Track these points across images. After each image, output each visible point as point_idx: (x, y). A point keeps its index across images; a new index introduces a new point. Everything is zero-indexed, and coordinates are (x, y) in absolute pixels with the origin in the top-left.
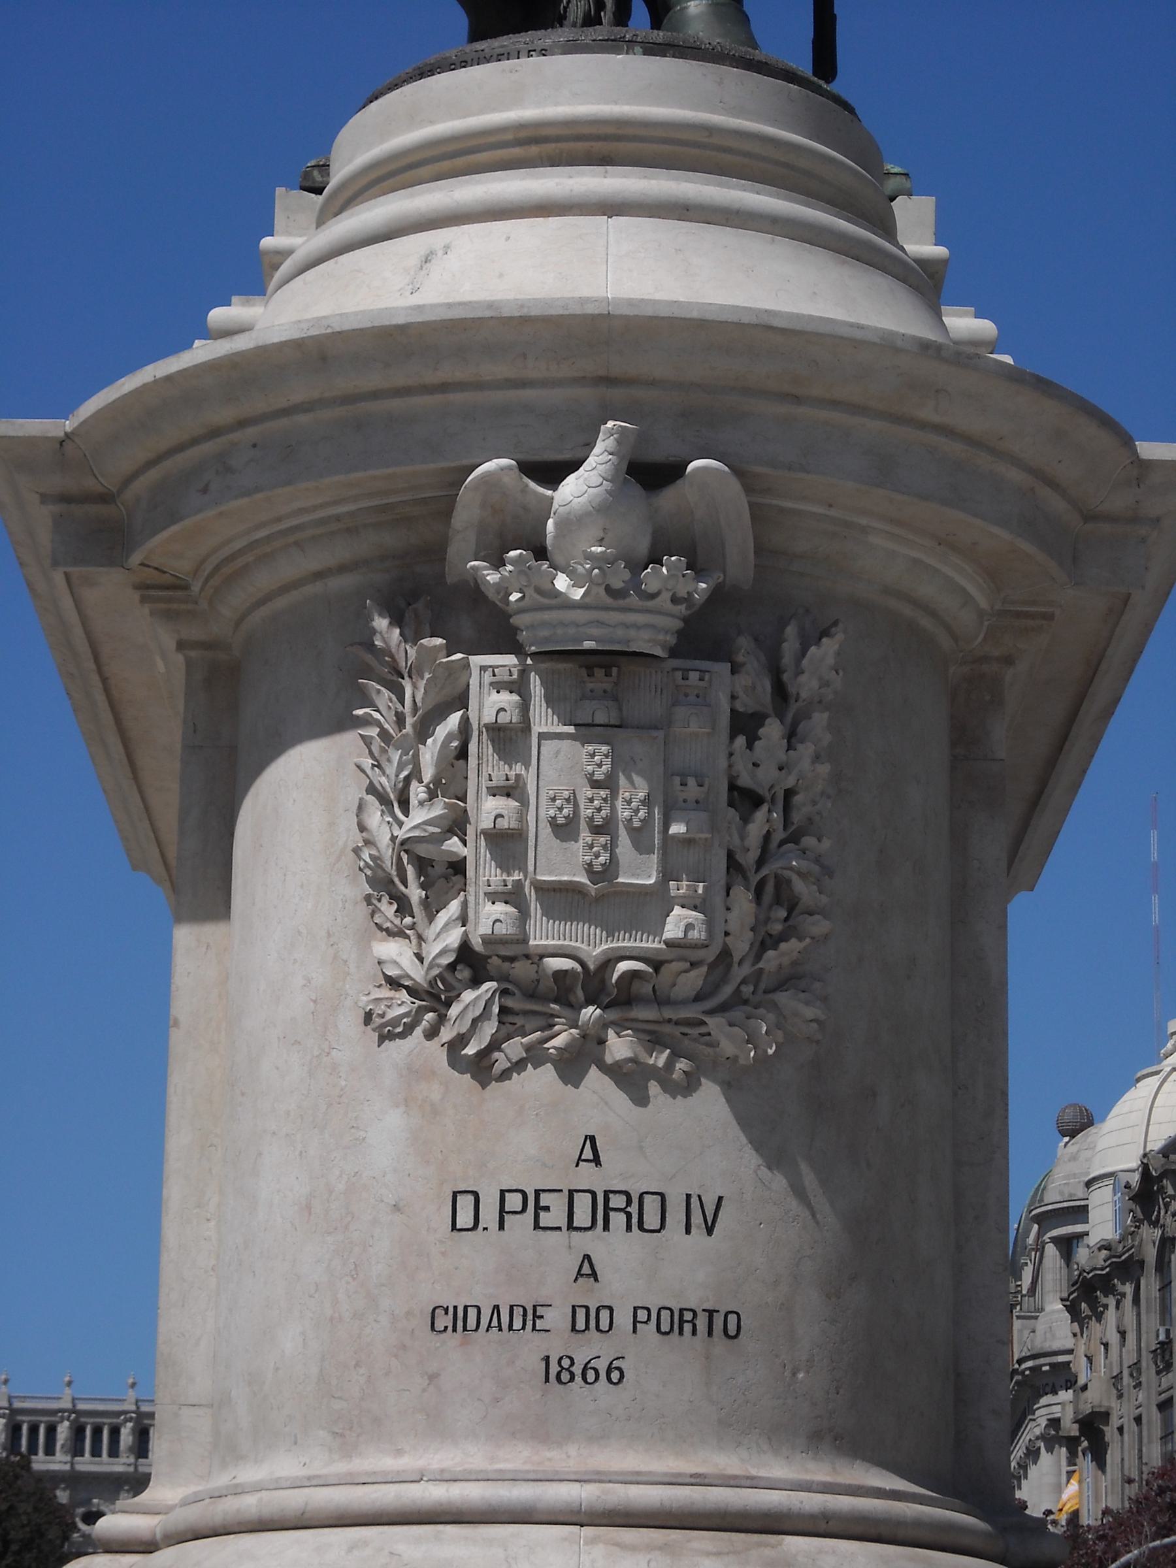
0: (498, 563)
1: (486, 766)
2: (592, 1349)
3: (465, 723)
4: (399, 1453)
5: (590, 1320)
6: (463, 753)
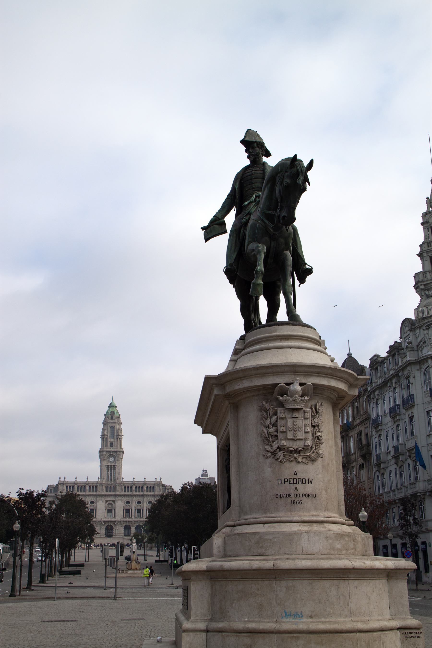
0: (282, 397)
1: (280, 423)
2: (297, 499)
3: (277, 417)
4: (272, 514)
5: (297, 496)
6: (277, 421)
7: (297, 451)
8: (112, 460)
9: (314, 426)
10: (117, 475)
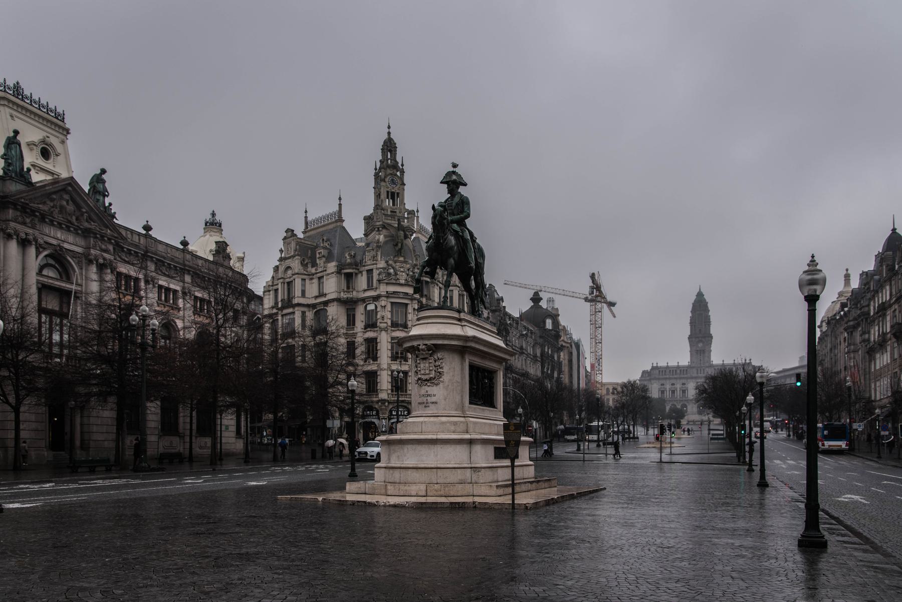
7: (426, 380)
8: (700, 345)
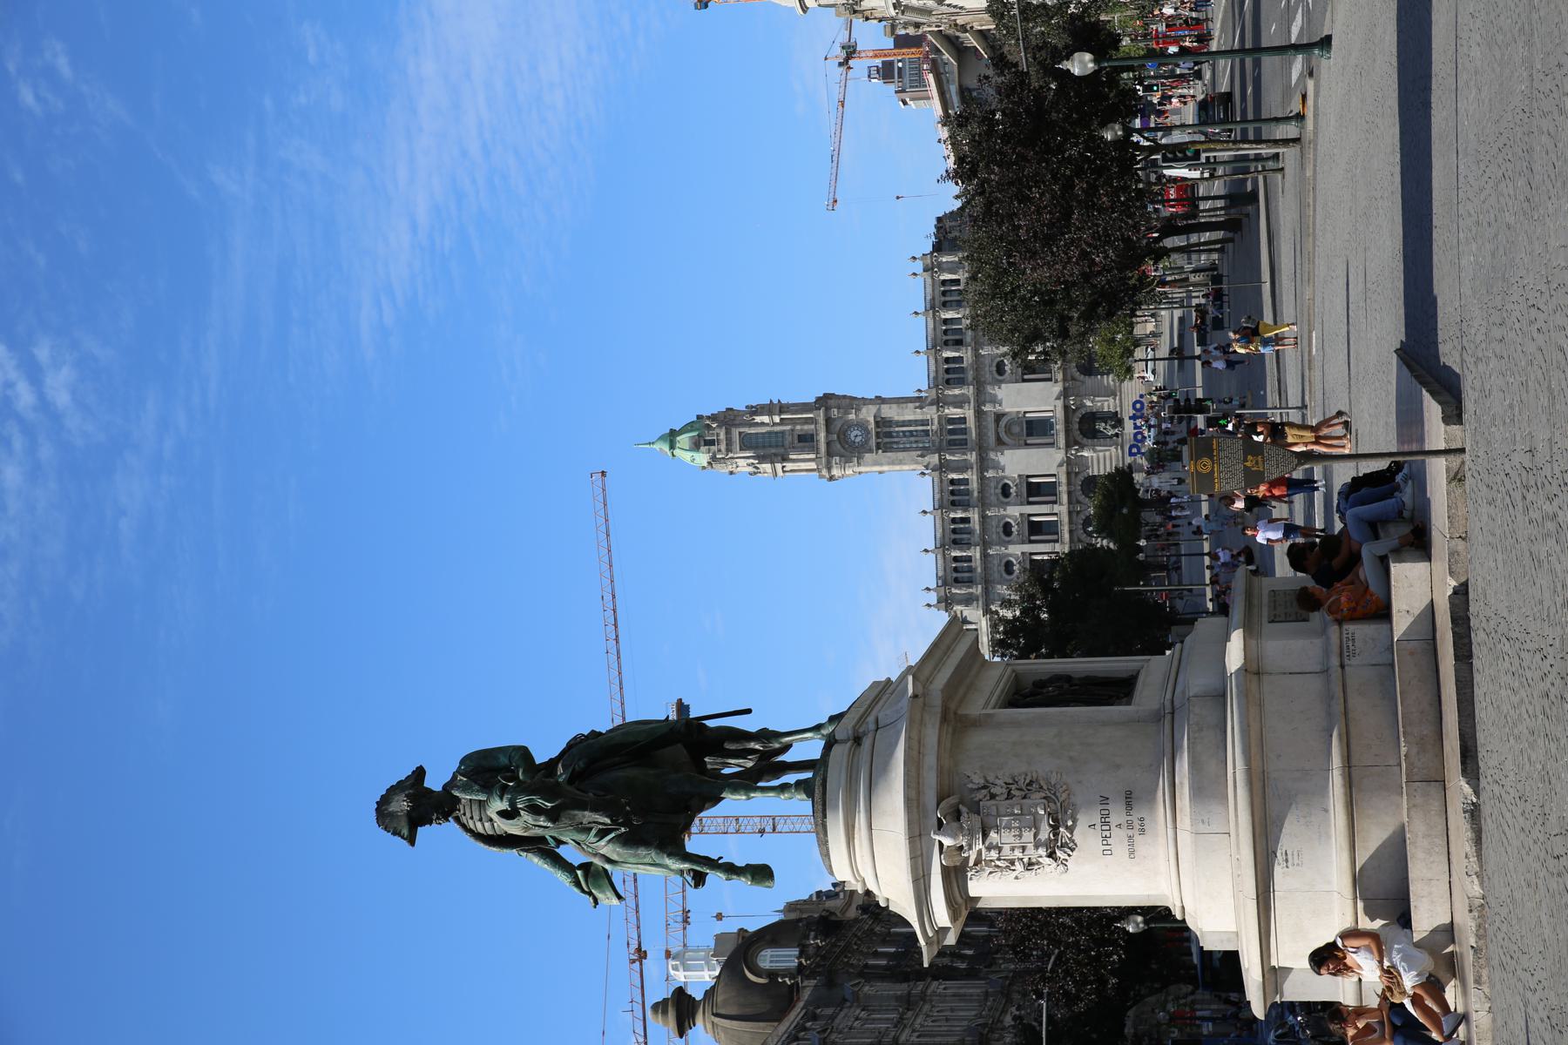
9: (1009, 796)
10: (910, 414)
